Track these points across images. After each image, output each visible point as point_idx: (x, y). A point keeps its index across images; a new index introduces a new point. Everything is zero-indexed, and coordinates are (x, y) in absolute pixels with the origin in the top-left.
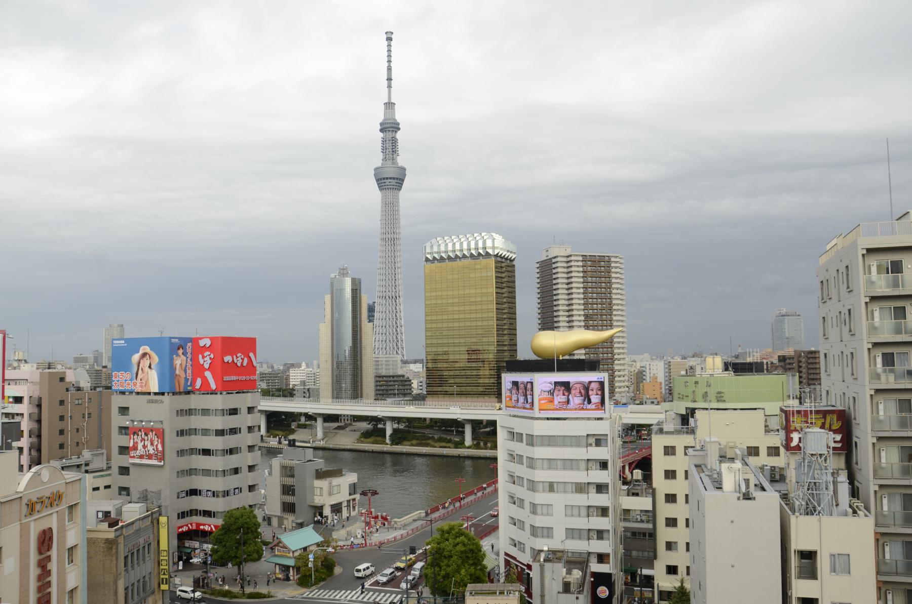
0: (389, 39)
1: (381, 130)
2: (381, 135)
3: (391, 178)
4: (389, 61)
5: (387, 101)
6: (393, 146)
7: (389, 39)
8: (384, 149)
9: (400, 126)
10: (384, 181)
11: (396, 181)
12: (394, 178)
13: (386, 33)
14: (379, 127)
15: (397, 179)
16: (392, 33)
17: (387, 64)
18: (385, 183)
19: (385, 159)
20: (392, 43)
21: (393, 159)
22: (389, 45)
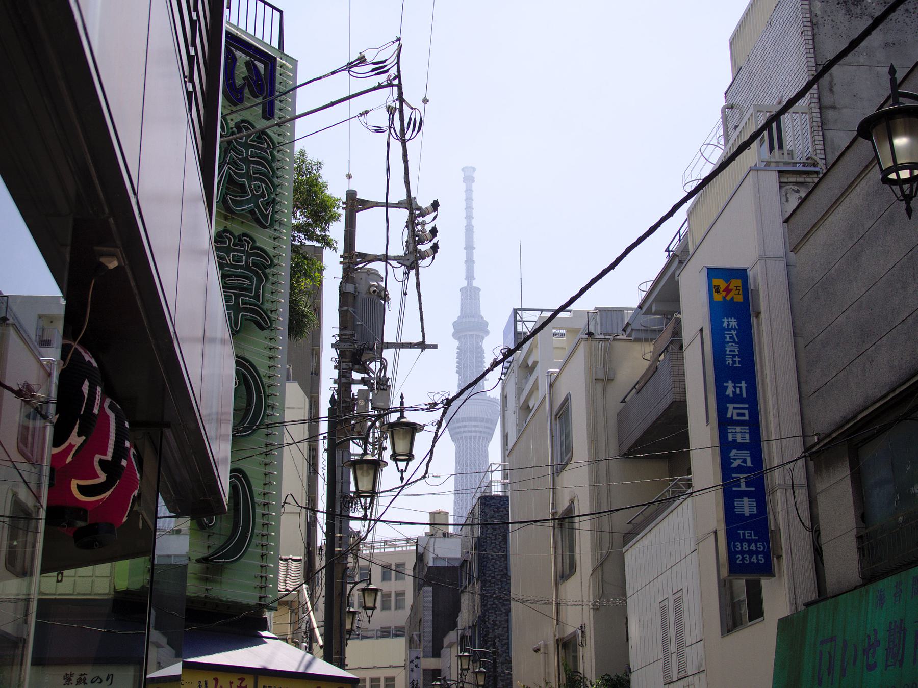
0: (469, 179)
1: (455, 335)
2: (456, 343)
3: (476, 419)
4: (469, 217)
5: (464, 284)
7: (469, 179)
10: (465, 424)
12: (482, 420)
13: (463, 170)
14: (453, 331)
15: (487, 421)
16: (474, 169)
17: (465, 222)
18: (465, 426)
20: (474, 186)
22: (469, 191)
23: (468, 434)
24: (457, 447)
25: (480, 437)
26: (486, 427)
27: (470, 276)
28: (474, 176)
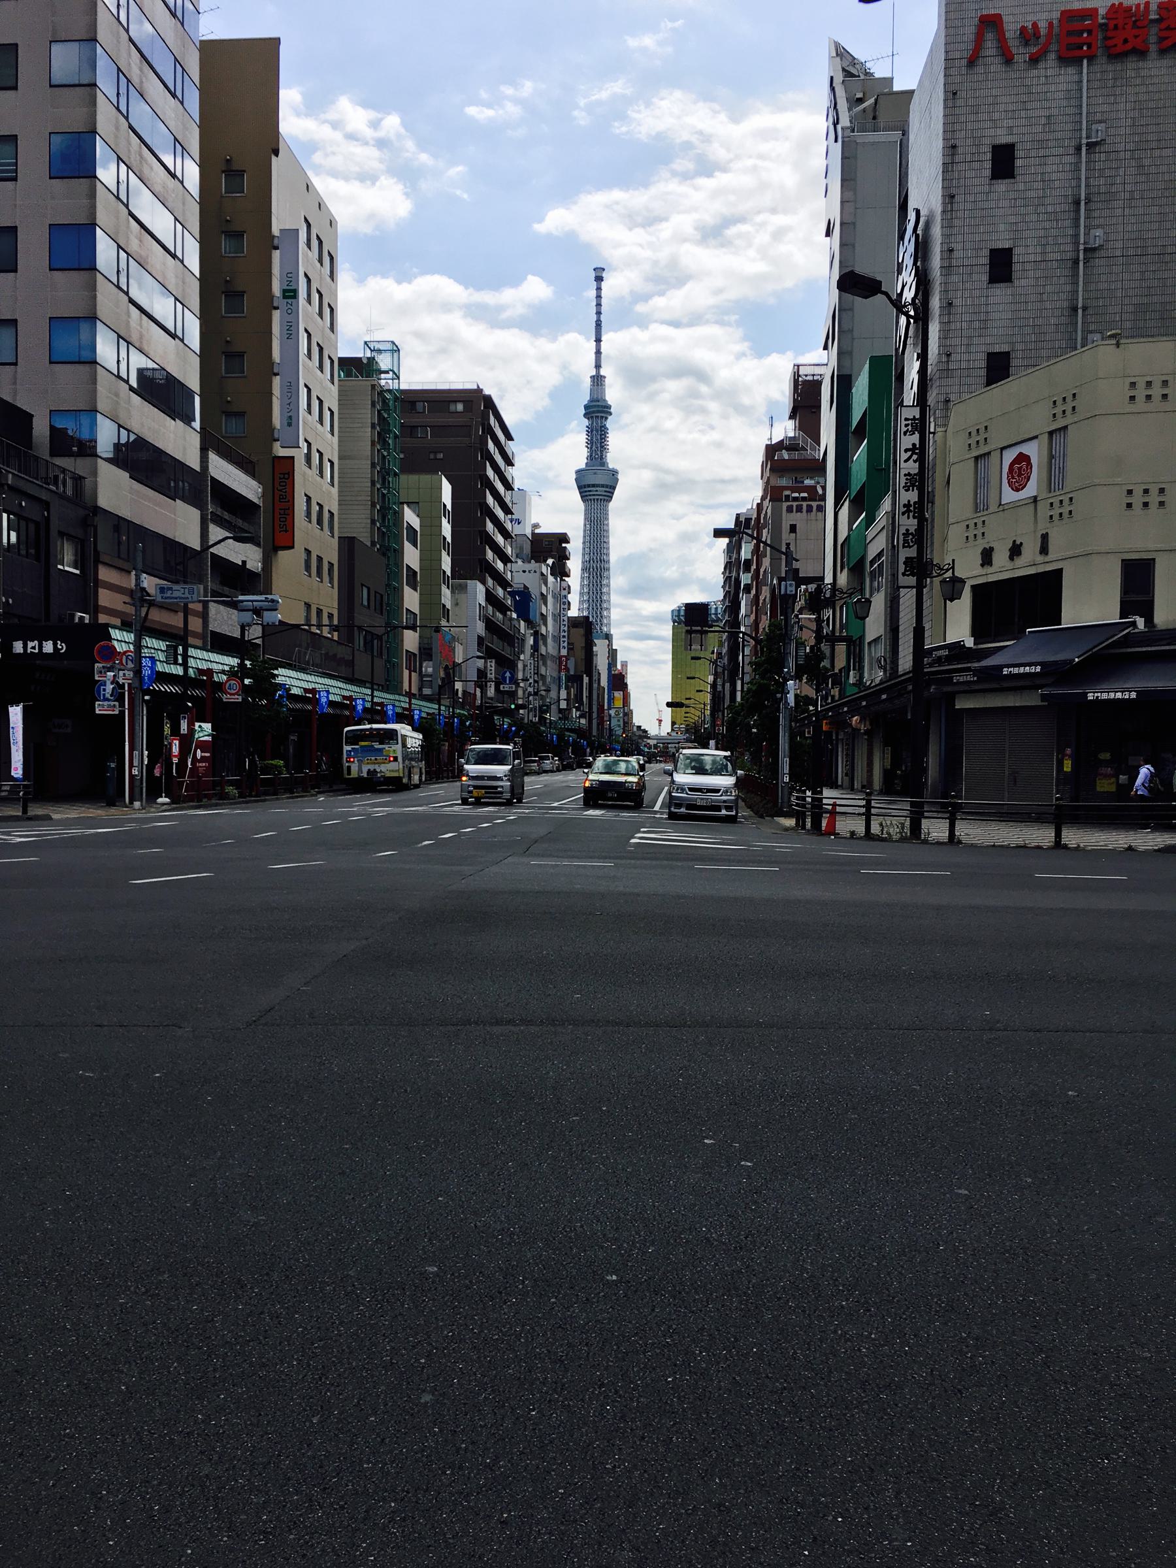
0: (599, 279)
2: (586, 422)
4: (599, 313)
5: (594, 374)
6: (601, 439)
8: (591, 444)
9: (612, 410)
10: (589, 489)
11: (604, 489)
12: (603, 486)
13: (594, 270)
15: (607, 486)
18: (590, 491)
19: (590, 457)
20: (603, 284)
21: (602, 458)
23: (592, 497)
24: (586, 507)
25: (601, 500)
26: (605, 491)
27: (598, 366)
28: (603, 275)
